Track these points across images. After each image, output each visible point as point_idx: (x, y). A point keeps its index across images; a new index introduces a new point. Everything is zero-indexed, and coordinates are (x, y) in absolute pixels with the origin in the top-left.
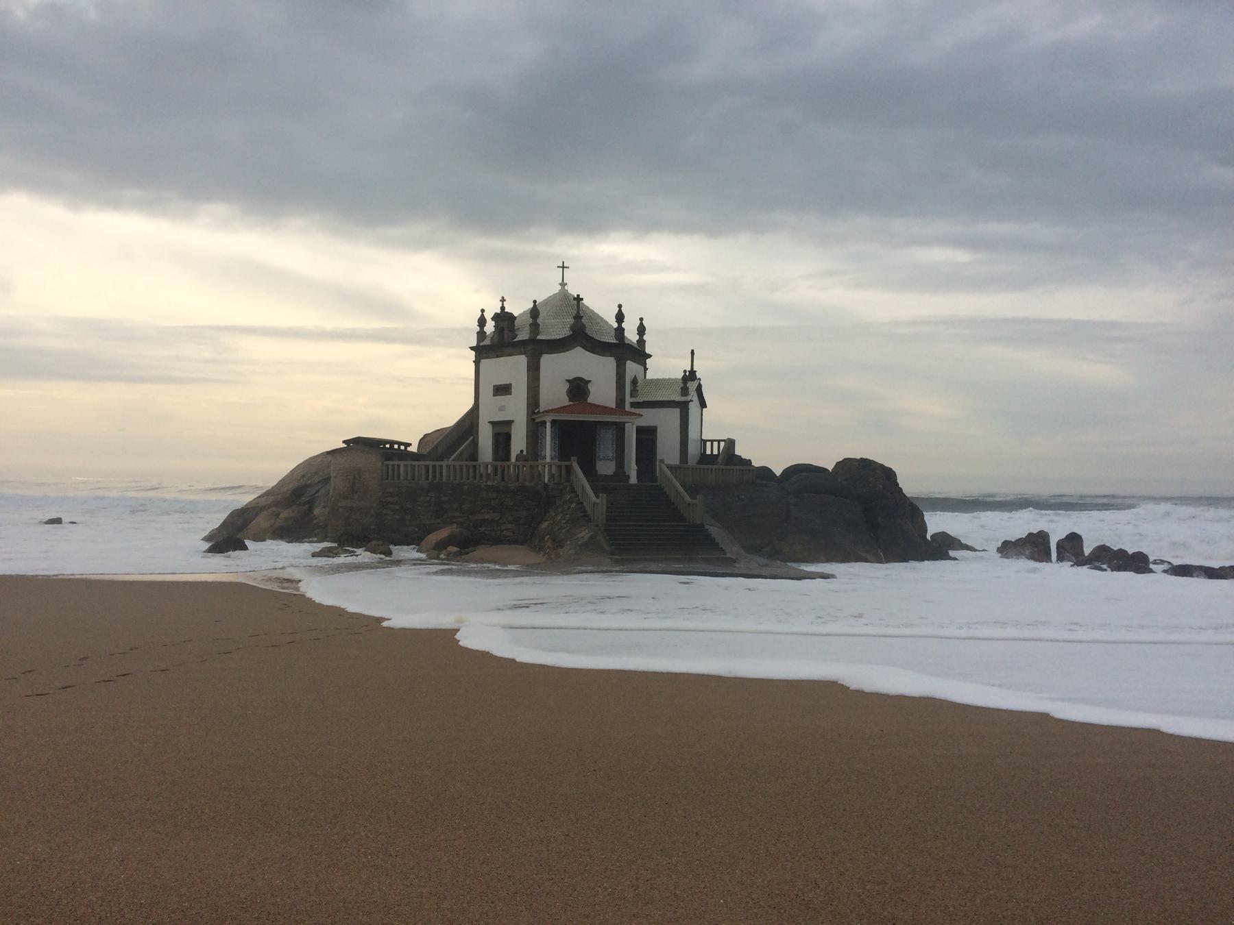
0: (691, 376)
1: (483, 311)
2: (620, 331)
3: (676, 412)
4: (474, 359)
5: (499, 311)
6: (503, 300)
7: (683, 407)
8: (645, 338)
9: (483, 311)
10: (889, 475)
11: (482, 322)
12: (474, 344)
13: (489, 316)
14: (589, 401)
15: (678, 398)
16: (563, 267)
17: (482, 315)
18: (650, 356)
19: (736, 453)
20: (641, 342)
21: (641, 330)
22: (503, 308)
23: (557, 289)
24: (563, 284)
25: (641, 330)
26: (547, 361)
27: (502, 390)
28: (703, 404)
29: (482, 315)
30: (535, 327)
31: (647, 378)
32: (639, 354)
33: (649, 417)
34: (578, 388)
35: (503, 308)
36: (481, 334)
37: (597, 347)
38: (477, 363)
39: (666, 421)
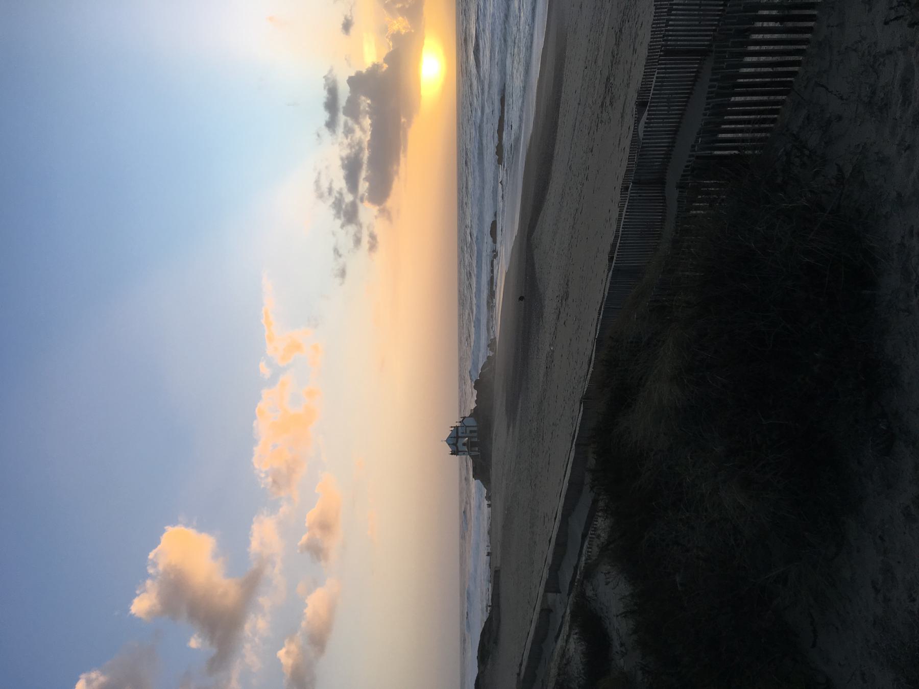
2: (454, 437)
3: (467, 428)
7: (467, 427)
14: (466, 442)
15: (465, 428)
20: (454, 427)
21: (452, 427)
23: (445, 442)
25: (452, 427)
26: (460, 450)
30: (454, 451)
32: (456, 428)
33: (468, 432)
34: (464, 444)
37: (457, 442)
39: (468, 429)
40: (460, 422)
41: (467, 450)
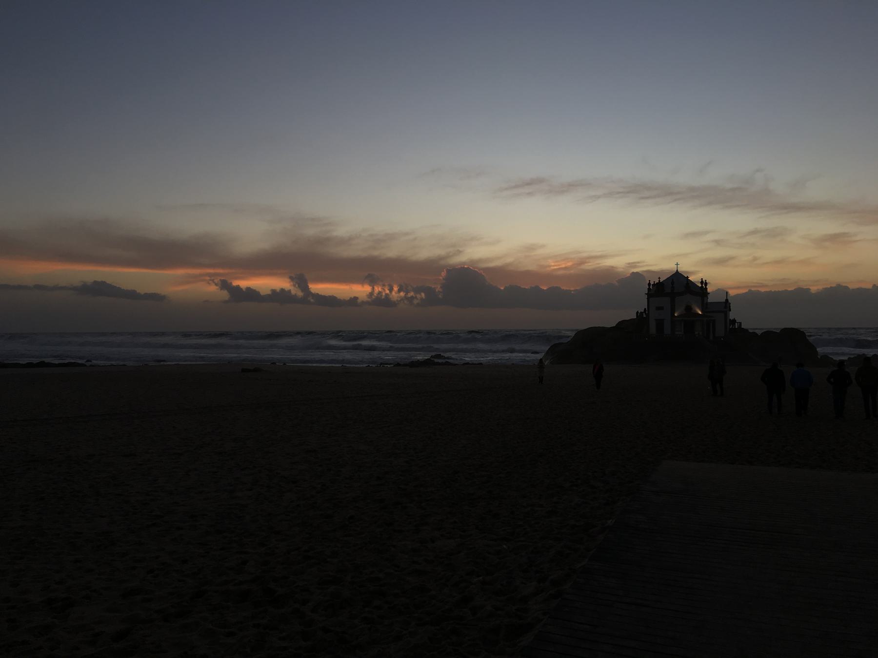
0: (727, 300)
1: (650, 281)
2: (702, 286)
4: (647, 297)
5: (658, 282)
6: (659, 278)
8: (707, 287)
9: (650, 281)
10: (803, 333)
11: (649, 284)
12: (647, 293)
13: (652, 283)
16: (677, 264)
17: (649, 283)
18: (709, 293)
19: (742, 327)
22: (659, 281)
24: (677, 270)
27: (659, 308)
28: (730, 310)
29: (649, 283)
31: (709, 301)
34: (689, 309)
35: (659, 281)
36: (649, 289)
38: (648, 299)
40: (727, 300)
41: (676, 315)
